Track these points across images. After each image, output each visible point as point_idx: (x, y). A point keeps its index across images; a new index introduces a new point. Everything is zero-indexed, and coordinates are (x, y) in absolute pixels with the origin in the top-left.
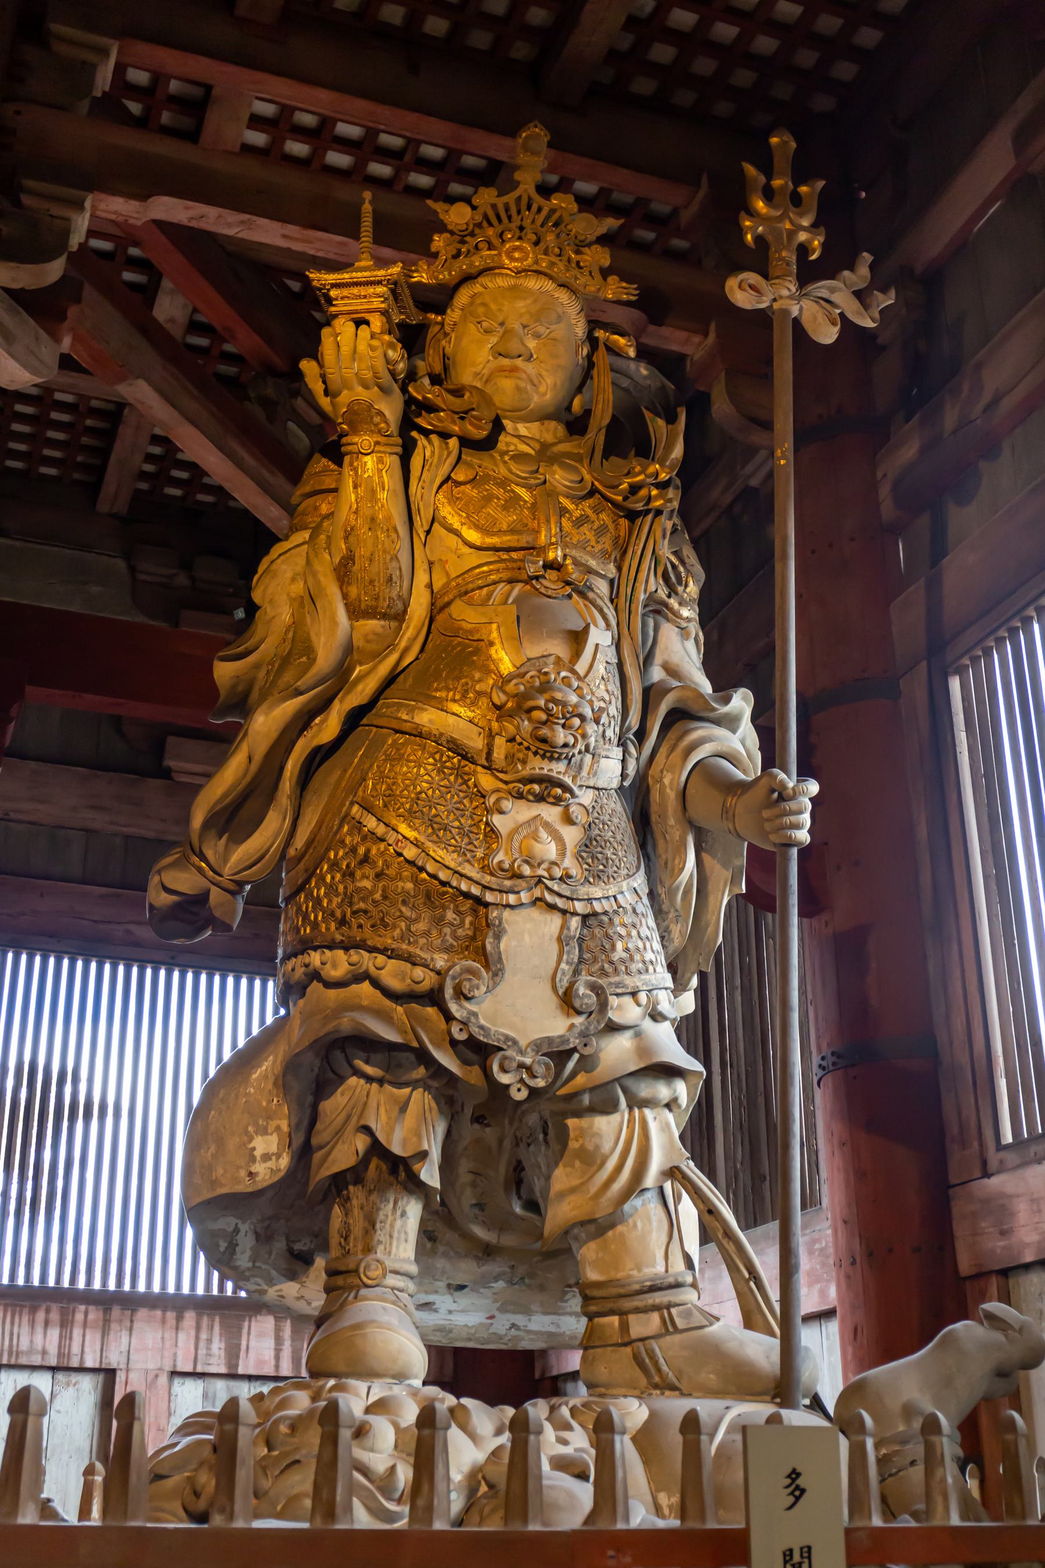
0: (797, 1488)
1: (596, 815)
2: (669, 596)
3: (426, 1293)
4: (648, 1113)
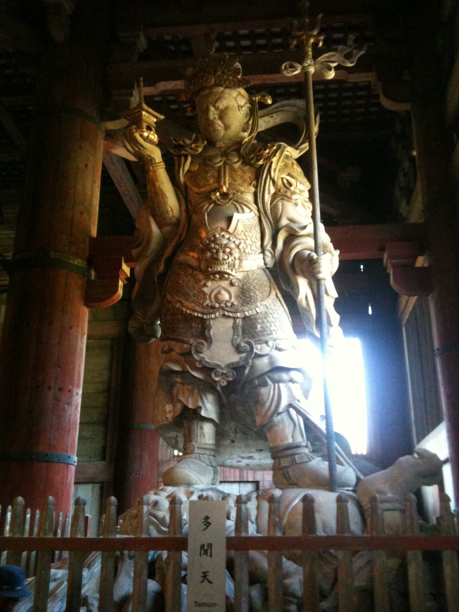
0: (208, 523)
1: (246, 281)
2: (286, 192)
3: (249, 453)
4: (282, 385)
